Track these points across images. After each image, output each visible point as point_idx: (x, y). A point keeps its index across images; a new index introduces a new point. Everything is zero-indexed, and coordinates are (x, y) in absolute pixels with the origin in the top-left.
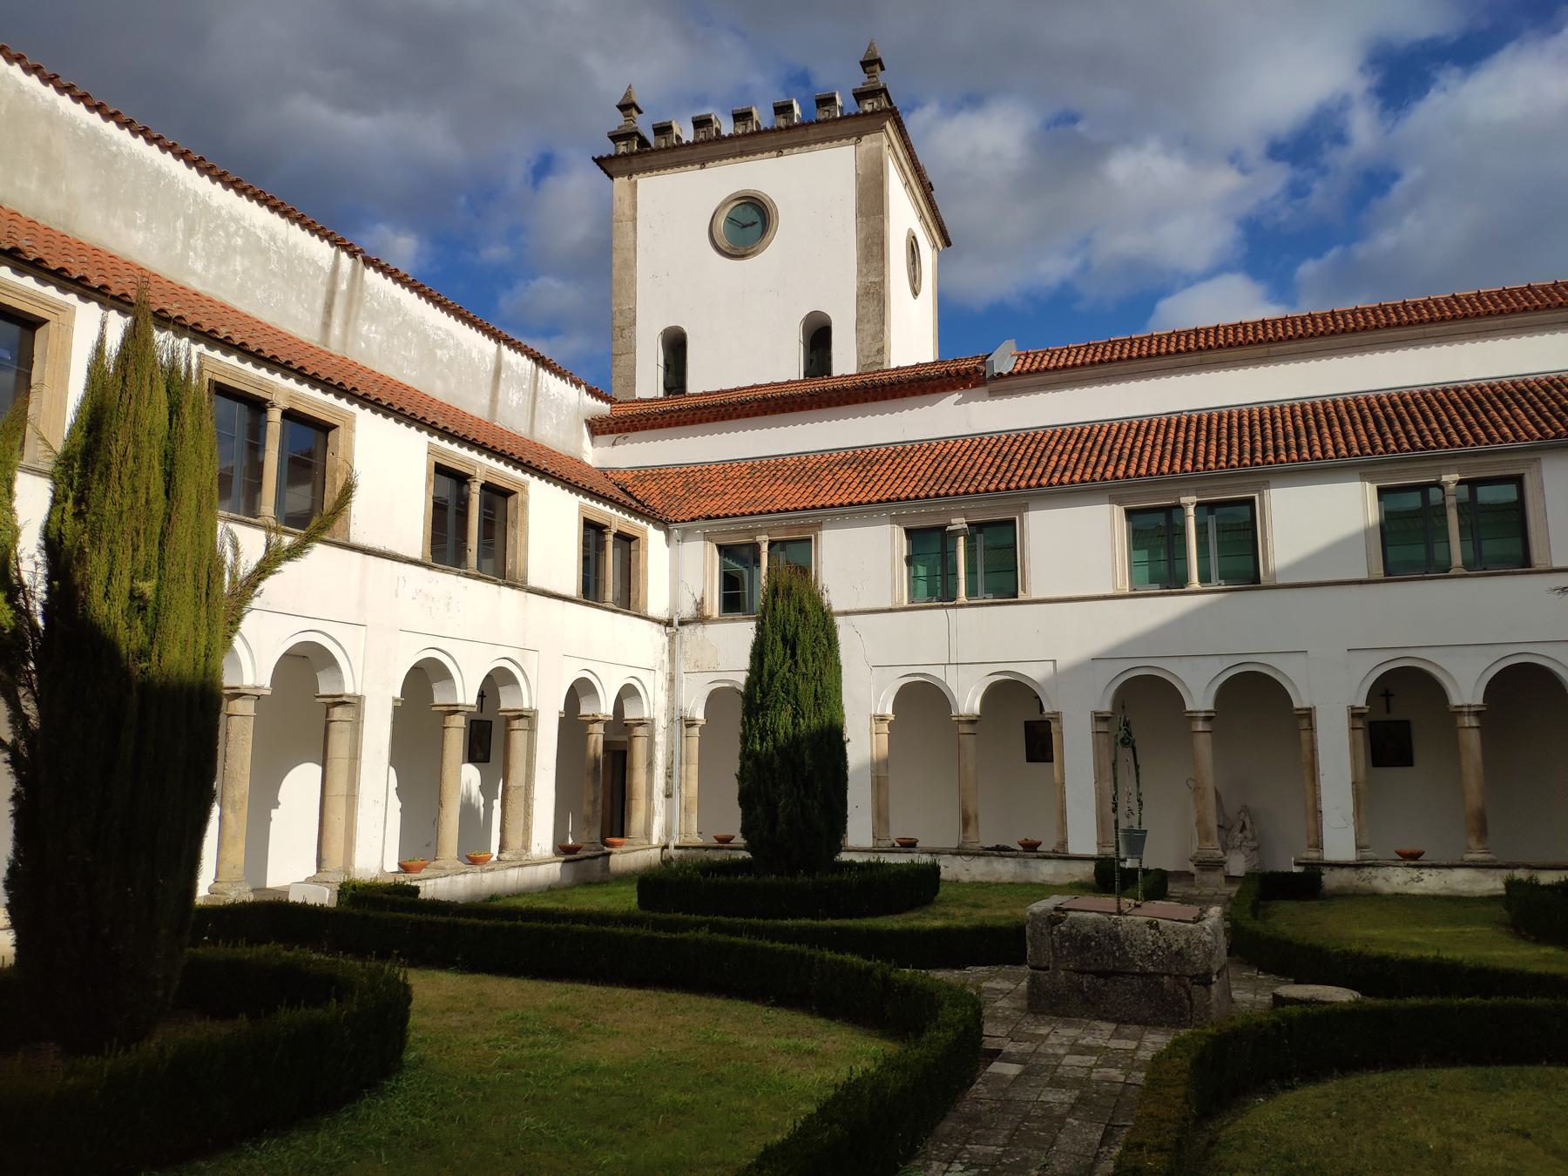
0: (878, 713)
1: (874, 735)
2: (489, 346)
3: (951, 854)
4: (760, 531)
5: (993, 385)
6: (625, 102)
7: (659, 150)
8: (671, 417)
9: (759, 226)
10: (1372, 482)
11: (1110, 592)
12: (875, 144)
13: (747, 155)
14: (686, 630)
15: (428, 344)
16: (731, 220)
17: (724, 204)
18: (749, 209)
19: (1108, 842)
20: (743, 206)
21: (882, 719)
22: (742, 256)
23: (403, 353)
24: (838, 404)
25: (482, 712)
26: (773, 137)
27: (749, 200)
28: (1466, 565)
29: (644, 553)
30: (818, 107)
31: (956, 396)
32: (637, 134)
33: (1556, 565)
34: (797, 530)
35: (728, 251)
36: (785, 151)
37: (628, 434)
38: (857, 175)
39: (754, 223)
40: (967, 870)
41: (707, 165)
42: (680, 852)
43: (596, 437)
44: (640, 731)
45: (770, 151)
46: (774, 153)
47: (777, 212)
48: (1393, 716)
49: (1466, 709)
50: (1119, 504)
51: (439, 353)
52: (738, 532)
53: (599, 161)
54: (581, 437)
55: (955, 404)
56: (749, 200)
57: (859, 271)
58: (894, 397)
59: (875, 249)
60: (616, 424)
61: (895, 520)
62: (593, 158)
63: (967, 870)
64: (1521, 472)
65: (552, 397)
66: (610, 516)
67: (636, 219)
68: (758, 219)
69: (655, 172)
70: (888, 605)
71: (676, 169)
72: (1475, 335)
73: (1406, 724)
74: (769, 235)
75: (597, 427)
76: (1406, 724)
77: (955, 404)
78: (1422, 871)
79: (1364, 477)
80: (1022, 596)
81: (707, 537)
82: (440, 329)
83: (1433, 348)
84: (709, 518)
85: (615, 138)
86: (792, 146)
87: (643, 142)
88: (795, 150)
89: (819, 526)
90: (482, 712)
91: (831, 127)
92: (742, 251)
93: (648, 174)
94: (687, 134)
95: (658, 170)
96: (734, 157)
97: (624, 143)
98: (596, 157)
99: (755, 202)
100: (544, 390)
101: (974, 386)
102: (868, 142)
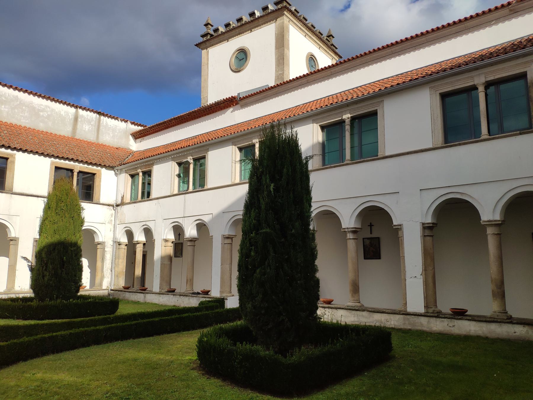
0: (165, 238)
1: (163, 247)
2: (73, 110)
3: (179, 295)
4: (136, 169)
5: (241, 103)
6: (207, 23)
7: (216, 37)
8: (153, 130)
9: (245, 59)
10: (317, 123)
11: (230, 183)
12: (281, 21)
13: (241, 34)
14: (119, 208)
15: (35, 112)
16: (237, 57)
17: (234, 53)
18: (242, 53)
19: (226, 291)
20: (240, 53)
21: (166, 241)
22: (239, 71)
23: (21, 114)
24: (197, 118)
25: (179, 240)
26: (248, 25)
27: (242, 50)
28: (352, 158)
29: (99, 179)
30: (263, 12)
31: (231, 109)
32: (209, 33)
33: (387, 154)
34: (148, 167)
35: (235, 70)
36: (253, 30)
37: (144, 138)
38: (276, 34)
39: (243, 59)
40: (183, 302)
41: (229, 40)
42: (112, 292)
43: (137, 140)
44: (99, 246)
45: (248, 31)
46: (250, 31)
47: (250, 53)
48: (374, 235)
49: (346, 230)
50: (235, 145)
51: (41, 113)
52: (133, 169)
53: (197, 45)
54: (129, 140)
55: (232, 112)
56: (242, 50)
57: (276, 70)
58: (213, 112)
59: (281, 61)
60: (140, 134)
61: (173, 159)
62: (195, 45)
63: (183, 302)
64: (375, 109)
65: (110, 126)
66: (74, 166)
67: (208, 64)
68: (244, 57)
69: (214, 46)
70: (169, 194)
71: (220, 44)
72: (414, 48)
73: (378, 238)
74: (247, 61)
75: (138, 136)
76: (378, 238)
77: (232, 112)
78: (326, 310)
79: (314, 121)
80: (206, 188)
81: (126, 172)
82: (42, 105)
83: (397, 57)
84: (124, 164)
85: (203, 36)
86: (255, 27)
87: (212, 35)
88: (256, 29)
89: (153, 164)
90: (179, 240)
91: (266, 18)
92: (239, 70)
93: (212, 47)
94: (222, 29)
95: (215, 45)
96: (237, 35)
97: (205, 38)
98: (195, 44)
99: (243, 51)
100: (105, 124)
101: (236, 104)
102: (279, 20)
